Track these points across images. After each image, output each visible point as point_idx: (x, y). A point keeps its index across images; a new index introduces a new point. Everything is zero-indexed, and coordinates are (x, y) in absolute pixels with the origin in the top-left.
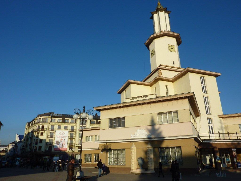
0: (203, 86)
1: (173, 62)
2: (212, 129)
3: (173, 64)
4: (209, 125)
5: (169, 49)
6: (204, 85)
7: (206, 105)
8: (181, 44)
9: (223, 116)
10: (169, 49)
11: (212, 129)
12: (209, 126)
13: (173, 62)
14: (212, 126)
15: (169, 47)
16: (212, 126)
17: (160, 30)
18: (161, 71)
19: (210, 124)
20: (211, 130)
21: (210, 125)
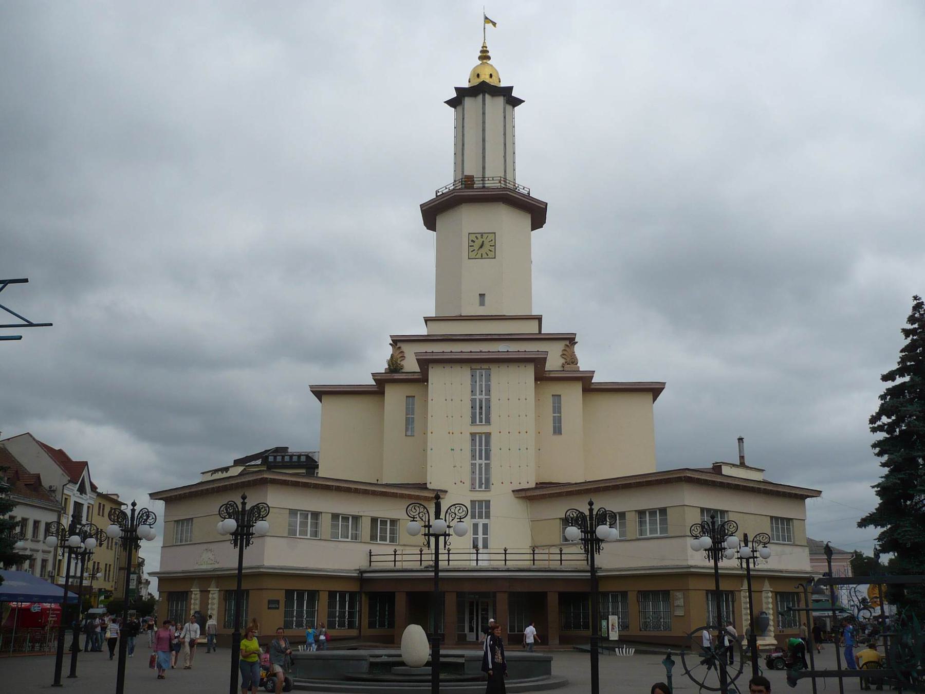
0: (481, 401)
1: (482, 296)
2: (485, 532)
3: (482, 303)
4: (476, 521)
5: (472, 249)
6: (484, 397)
7: (478, 462)
8: (65, 450)
9: (529, 494)
10: (472, 249)
11: (485, 532)
12: (476, 526)
13: (482, 296)
14: (485, 526)
15: (472, 244)
16: (485, 526)
17: (463, 172)
18: (400, 348)
19: (480, 517)
20: (480, 536)
21: (481, 522)
